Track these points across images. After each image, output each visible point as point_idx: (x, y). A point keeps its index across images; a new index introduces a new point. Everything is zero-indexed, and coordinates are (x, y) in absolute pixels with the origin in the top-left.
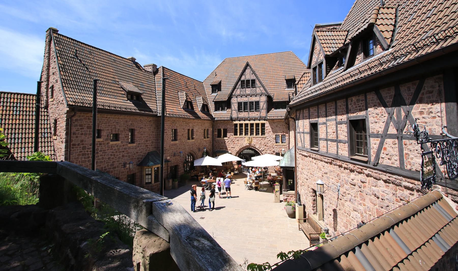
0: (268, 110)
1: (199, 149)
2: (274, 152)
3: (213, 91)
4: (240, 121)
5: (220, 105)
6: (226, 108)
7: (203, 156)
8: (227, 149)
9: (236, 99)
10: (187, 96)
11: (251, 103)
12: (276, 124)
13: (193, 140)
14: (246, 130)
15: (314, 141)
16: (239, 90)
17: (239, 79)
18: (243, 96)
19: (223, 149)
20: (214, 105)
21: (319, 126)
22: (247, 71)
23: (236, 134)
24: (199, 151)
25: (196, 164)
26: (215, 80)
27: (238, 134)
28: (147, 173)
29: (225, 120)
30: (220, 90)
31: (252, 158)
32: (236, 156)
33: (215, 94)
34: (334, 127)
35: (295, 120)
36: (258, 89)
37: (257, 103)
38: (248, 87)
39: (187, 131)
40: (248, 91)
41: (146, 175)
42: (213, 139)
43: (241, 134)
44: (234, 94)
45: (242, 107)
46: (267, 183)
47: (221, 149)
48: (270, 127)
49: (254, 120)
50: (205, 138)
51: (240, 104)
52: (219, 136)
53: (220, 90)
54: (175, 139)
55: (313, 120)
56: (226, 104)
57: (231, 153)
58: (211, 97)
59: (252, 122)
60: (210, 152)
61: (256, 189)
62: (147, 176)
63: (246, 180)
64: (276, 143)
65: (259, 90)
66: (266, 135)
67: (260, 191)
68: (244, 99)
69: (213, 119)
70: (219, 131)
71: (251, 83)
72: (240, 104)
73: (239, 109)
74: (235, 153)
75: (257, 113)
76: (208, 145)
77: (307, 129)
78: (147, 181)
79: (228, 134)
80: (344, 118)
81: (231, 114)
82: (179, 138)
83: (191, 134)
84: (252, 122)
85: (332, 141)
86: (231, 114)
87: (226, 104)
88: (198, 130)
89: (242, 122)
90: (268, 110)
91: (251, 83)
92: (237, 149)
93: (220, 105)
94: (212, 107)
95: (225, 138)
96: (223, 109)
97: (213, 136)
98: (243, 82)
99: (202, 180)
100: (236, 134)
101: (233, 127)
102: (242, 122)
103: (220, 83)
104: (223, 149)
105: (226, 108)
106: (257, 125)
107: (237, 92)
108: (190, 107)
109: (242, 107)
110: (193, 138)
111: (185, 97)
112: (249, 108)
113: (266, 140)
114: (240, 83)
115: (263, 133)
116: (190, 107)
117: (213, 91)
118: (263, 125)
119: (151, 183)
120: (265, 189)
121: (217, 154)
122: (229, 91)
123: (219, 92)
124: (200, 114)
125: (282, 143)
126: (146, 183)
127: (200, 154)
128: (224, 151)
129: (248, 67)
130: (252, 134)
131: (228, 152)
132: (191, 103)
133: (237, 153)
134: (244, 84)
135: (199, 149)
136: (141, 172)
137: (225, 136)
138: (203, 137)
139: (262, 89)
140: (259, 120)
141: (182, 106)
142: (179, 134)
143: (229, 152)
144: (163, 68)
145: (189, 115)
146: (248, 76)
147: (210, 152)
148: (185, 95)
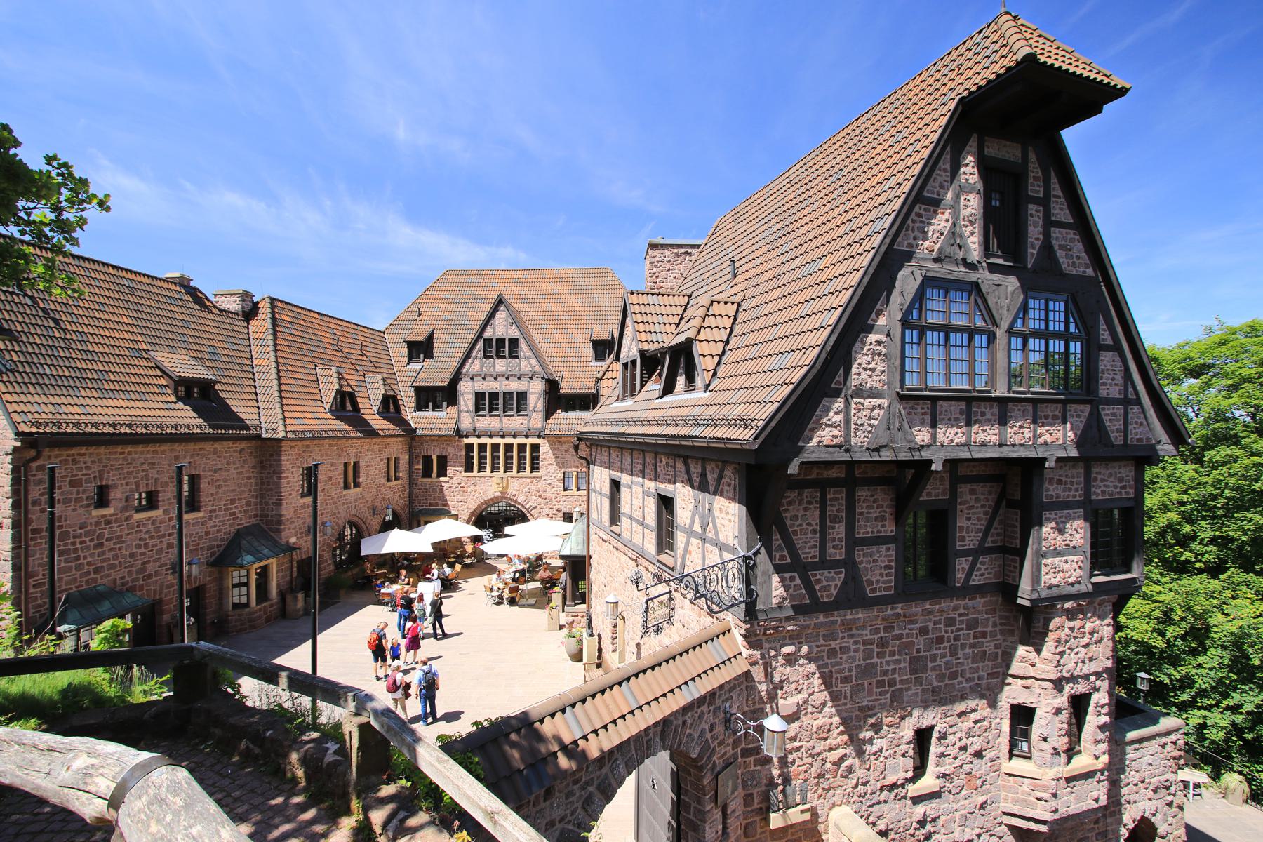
0: (548, 414)
1: (374, 511)
2: (559, 510)
3: (412, 358)
4: (479, 437)
5: (428, 397)
6: (445, 404)
7: (386, 527)
8: (446, 505)
9: (470, 383)
10: (340, 377)
11: (508, 395)
12: (566, 446)
13: (358, 490)
14: (495, 460)
15: (615, 518)
16: (477, 362)
17: (480, 335)
18: (487, 375)
19: (437, 504)
20: (413, 394)
21: (623, 489)
22: (498, 315)
23: (469, 468)
24: (374, 513)
25: (369, 547)
26: (416, 329)
27: (475, 468)
28: (236, 581)
29: (440, 436)
30: (429, 355)
31: (508, 530)
32: (468, 522)
33: (415, 366)
34: (640, 496)
35: (588, 464)
36: (524, 362)
37: (522, 396)
38: (500, 355)
39: (341, 468)
40: (501, 365)
41: (234, 586)
42: (411, 481)
43: (482, 468)
44: (464, 370)
45: (486, 403)
46: (538, 585)
47: (431, 505)
48: (550, 454)
49: (515, 436)
50: (389, 480)
51: (479, 396)
52: (427, 473)
53: (429, 355)
55: (616, 475)
56: (444, 395)
57: (456, 517)
58: (408, 375)
59: (509, 440)
60: (404, 514)
61: (513, 602)
62: (236, 591)
63: (490, 581)
64: (565, 490)
65: (527, 363)
66: (542, 472)
67: (523, 606)
68: (489, 386)
69: (410, 432)
70: (427, 461)
71: (506, 348)
72: (479, 396)
73: (478, 408)
74: (465, 515)
75: (520, 420)
76: (397, 498)
77: (606, 489)
78: (236, 600)
79: (450, 470)
80: (650, 485)
81: (458, 419)
83: (352, 475)
84: (509, 440)
85: (637, 521)
86: (458, 419)
87: (444, 395)
88: (372, 459)
89: (483, 440)
90: (548, 414)
91: (506, 348)
92: (473, 504)
93: (428, 397)
94: (408, 401)
95: (442, 479)
96: (437, 407)
97: (410, 473)
98: (488, 342)
99: (383, 591)
100: (469, 468)
101: (463, 452)
102: (483, 440)
103: (430, 337)
104: (437, 504)
105: (445, 404)
106: (522, 448)
107: (474, 366)
108: (349, 406)
109: (486, 403)
111: (336, 381)
112: (501, 406)
113: (542, 482)
114: (480, 344)
115: (535, 467)
116: (349, 406)
117: (412, 358)
118: (536, 448)
119: (247, 605)
120: (532, 601)
121: (423, 519)
122: (455, 363)
123: (427, 362)
124: (378, 423)
125: (578, 489)
126: (236, 606)
127: (376, 522)
128: (439, 511)
129: (502, 308)
130: (508, 468)
131: (447, 514)
132: (352, 396)
133: (472, 514)
134: (491, 347)
135: (374, 511)
136: (220, 580)
137: (442, 473)
138: (384, 480)
139: (534, 361)
140: (527, 437)
141: (328, 406)
143: (453, 512)
144: (273, 300)
145: (347, 427)
146: (501, 328)
147: (404, 514)
148: (335, 375)
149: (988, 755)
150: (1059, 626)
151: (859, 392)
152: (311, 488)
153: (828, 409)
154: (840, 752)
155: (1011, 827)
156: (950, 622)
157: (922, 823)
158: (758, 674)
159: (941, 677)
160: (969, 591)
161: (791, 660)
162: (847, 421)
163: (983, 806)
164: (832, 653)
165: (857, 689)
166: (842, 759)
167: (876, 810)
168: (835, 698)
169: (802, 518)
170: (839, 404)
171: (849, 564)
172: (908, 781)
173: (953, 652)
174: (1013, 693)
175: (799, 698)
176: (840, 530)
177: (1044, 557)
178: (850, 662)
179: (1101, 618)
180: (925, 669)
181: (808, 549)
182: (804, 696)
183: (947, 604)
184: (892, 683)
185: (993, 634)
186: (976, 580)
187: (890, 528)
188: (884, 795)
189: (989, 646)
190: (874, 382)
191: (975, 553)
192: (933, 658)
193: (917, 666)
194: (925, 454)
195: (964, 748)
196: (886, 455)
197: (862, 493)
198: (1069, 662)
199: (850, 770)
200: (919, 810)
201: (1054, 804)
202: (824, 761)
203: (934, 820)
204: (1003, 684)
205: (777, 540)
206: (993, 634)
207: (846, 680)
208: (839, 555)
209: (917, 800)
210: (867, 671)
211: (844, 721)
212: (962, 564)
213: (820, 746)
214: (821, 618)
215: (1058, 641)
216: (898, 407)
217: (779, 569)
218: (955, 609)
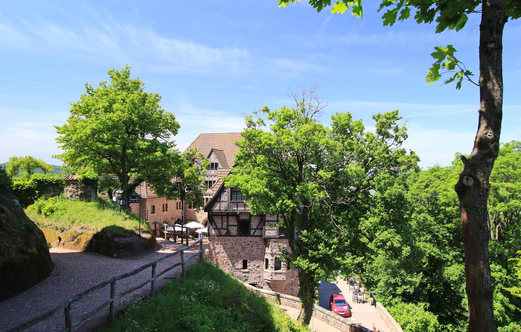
22: (212, 155)
40: (213, 172)
50: (177, 209)
57: (199, 222)
74: (201, 221)
82: (156, 211)
83: (165, 208)
110: (167, 211)
133: (204, 221)
142: (156, 208)
146: (213, 159)
149: (261, 267)
150: (272, 244)
151: (222, 202)
156: (251, 241)
157: (245, 276)
158: (211, 245)
159: (249, 251)
160: (253, 236)
161: (217, 244)
164: (225, 244)
165: (230, 251)
167: (235, 273)
168: (226, 251)
169: (218, 221)
171: (227, 229)
174: (266, 257)
176: (225, 223)
178: (229, 246)
179: (284, 243)
181: (219, 226)
186: (256, 234)
187: (236, 224)
189: (260, 247)
190: (225, 200)
191: (256, 229)
193: (243, 248)
195: (255, 265)
196: (228, 211)
197: (230, 217)
198: (274, 251)
199: (229, 264)
200: (244, 274)
205: (213, 224)
208: (225, 227)
209: (244, 272)
210: (232, 248)
211: (228, 256)
212: (252, 232)
213: (223, 259)
217: (214, 229)
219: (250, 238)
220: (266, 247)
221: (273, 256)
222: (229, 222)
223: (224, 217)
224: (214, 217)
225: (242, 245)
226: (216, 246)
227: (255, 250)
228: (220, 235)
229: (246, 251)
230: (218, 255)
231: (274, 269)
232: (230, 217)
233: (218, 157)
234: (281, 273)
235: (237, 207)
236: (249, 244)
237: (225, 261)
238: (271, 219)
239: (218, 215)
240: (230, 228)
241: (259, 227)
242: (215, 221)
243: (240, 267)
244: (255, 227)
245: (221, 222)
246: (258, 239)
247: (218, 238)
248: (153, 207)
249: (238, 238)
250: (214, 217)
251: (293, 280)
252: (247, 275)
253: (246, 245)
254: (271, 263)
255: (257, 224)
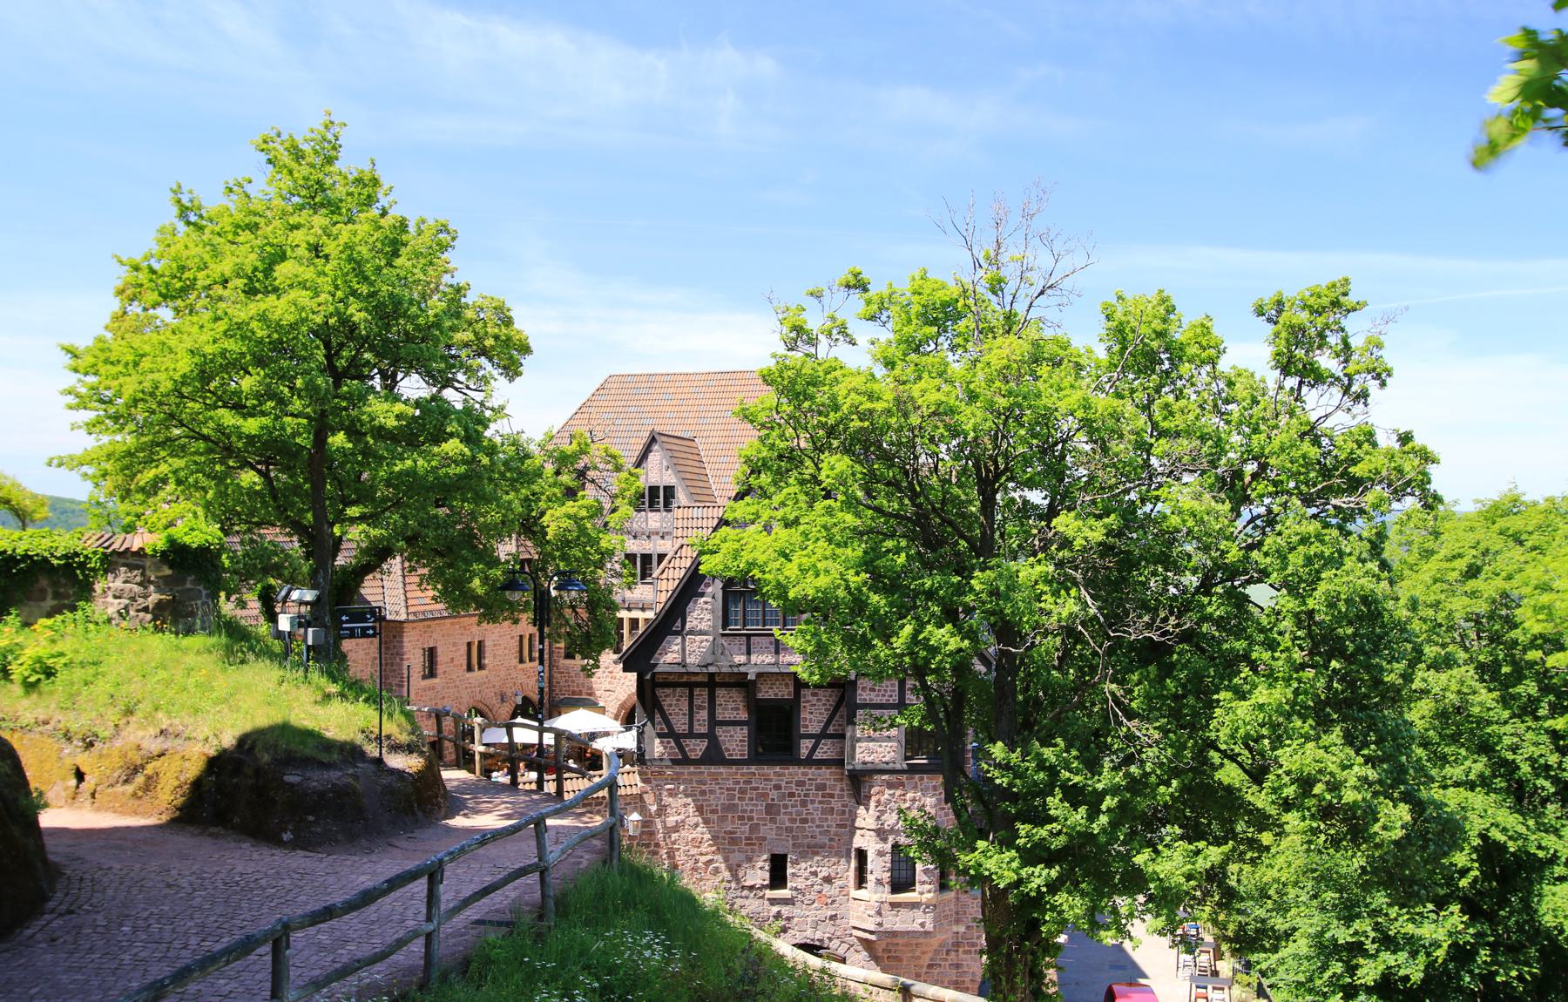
1: (503, 698)
4: (629, 609)
22: (651, 456)
39: (464, 649)
40: (654, 520)
54: (431, 672)
57: (603, 710)
74: (612, 708)
82: (440, 669)
83: (476, 657)
110: (481, 667)
129: (656, 447)
133: (622, 706)
135: (503, 698)
142: (442, 657)
146: (657, 472)
149: (838, 883)
150: (880, 793)
151: (691, 632)
152: (431, 672)
153: (669, 643)
154: (709, 857)
155: (860, 939)
156: (800, 784)
157: (778, 916)
158: (649, 798)
159: (793, 821)
160: (810, 762)
161: (672, 793)
162: (684, 649)
163: (833, 918)
164: (703, 793)
165: (723, 819)
166: (711, 861)
167: (739, 902)
168: (706, 822)
169: (675, 705)
170: (679, 640)
171: (711, 736)
172: (763, 887)
173: (804, 804)
174: (858, 842)
175: (679, 818)
176: (704, 714)
177: (859, 740)
178: (718, 799)
179: (924, 792)
180: (778, 813)
181: (680, 725)
182: (682, 817)
183: (793, 769)
184: (751, 819)
185: (841, 796)
186: (818, 755)
187: (744, 716)
188: (745, 893)
189: (836, 804)
190: (703, 626)
191: (818, 738)
192: (786, 806)
193: (771, 810)
194: (742, 669)
195: (815, 874)
196: (712, 669)
197: (720, 692)
198: (891, 819)
200: (775, 909)
201: (879, 920)
202: (697, 862)
203: (788, 919)
204: (852, 834)
205: (658, 718)
206: (841, 796)
207: (714, 812)
208: (704, 730)
209: (773, 902)
210: (731, 808)
211: (714, 838)
212: (805, 746)
213: (694, 851)
214: (692, 769)
215: (878, 802)
216: (723, 641)
217: (660, 735)
218: (804, 774)
219: (796, 772)
220: (859, 803)
221: (885, 840)
222: (719, 710)
223: (697, 691)
224: (660, 692)
225: (765, 795)
226: (667, 800)
227: (817, 815)
228: (685, 761)
229: (783, 819)
230: (674, 836)
231: (888, 888)
232: (720, 692)
233: (675, 463)
234: (914, 905)
235: (749, 653)
236: (792, 795)
237: (704, 859)
238: (877, 700)
239: (675, 685)
240: (719, 731)
241: (831, 730)
242: (665, 705)
243: (759, 882)
244: (815, 728)
245: (686, 709)
246: (826, 774)
247: (678, 769)
248: (431, 654)
249: (753, 769)
250: (660, 692)
251: (962, 929)
252: (785, 910)
253: (782, 797)
254: (878, 867)
255: (825, 717)
